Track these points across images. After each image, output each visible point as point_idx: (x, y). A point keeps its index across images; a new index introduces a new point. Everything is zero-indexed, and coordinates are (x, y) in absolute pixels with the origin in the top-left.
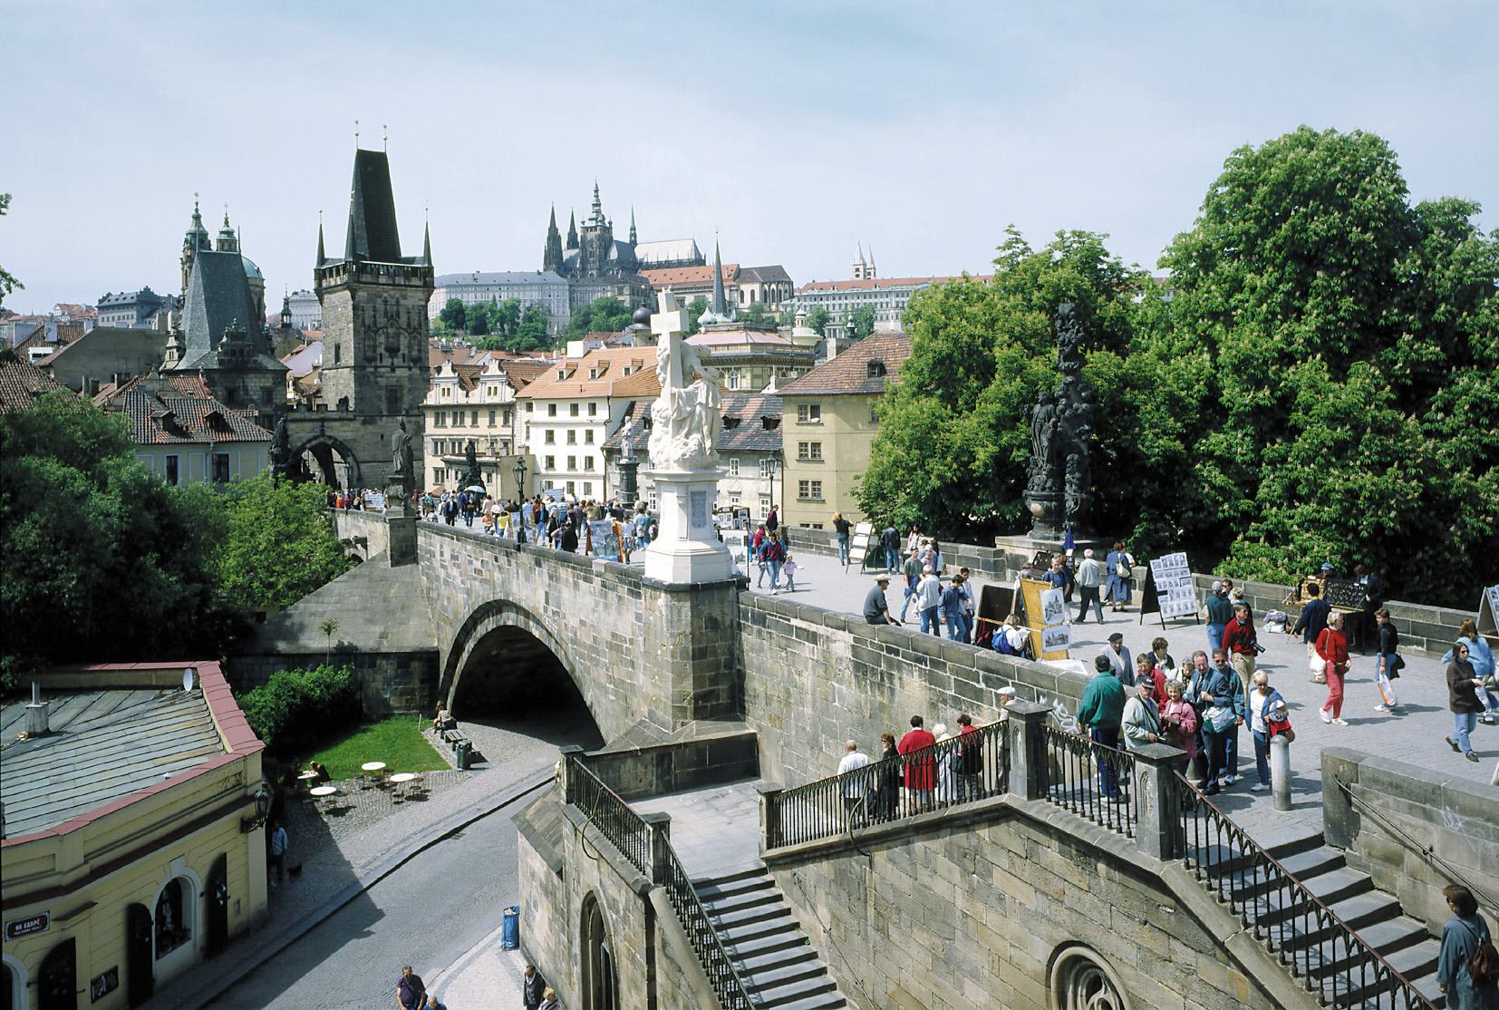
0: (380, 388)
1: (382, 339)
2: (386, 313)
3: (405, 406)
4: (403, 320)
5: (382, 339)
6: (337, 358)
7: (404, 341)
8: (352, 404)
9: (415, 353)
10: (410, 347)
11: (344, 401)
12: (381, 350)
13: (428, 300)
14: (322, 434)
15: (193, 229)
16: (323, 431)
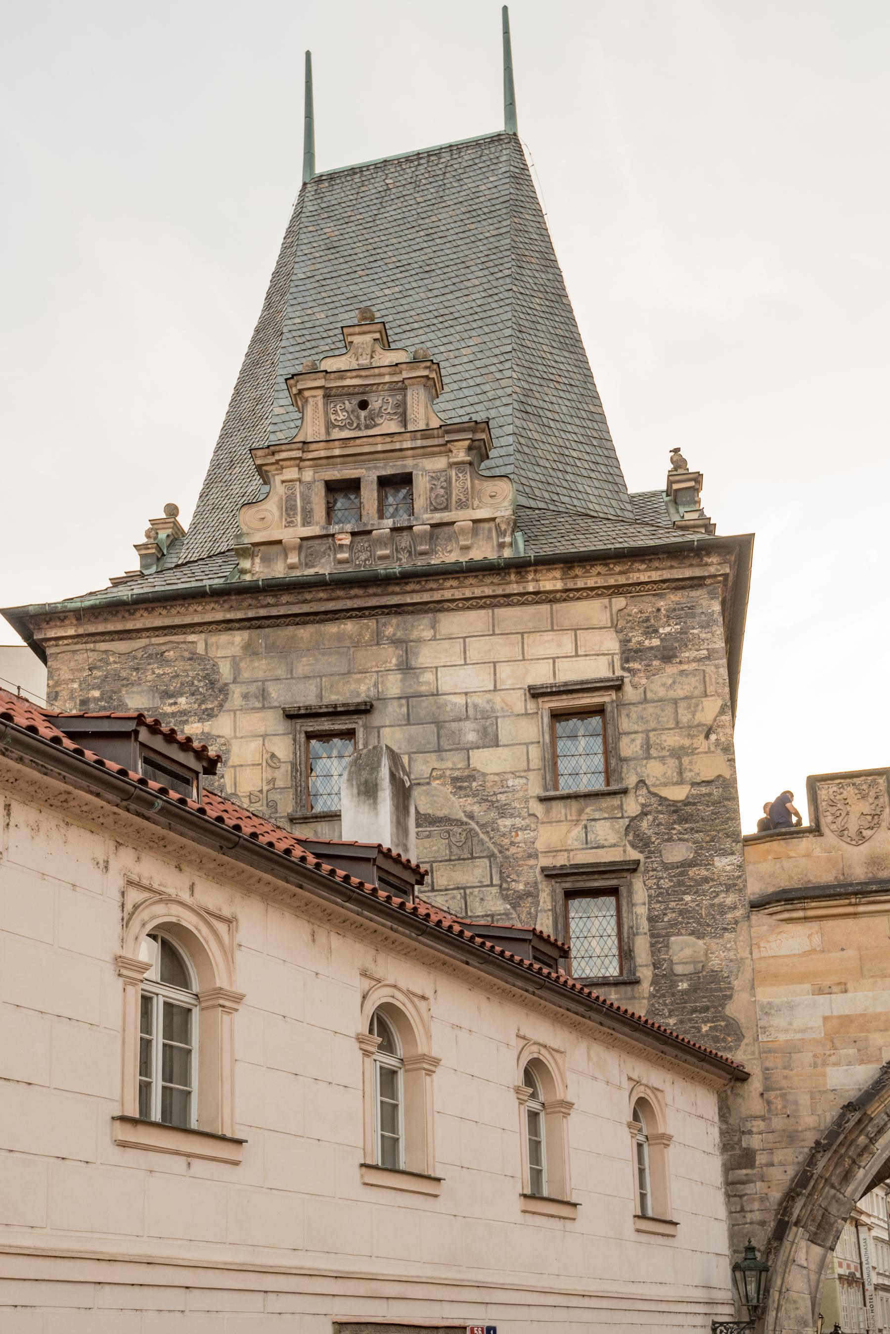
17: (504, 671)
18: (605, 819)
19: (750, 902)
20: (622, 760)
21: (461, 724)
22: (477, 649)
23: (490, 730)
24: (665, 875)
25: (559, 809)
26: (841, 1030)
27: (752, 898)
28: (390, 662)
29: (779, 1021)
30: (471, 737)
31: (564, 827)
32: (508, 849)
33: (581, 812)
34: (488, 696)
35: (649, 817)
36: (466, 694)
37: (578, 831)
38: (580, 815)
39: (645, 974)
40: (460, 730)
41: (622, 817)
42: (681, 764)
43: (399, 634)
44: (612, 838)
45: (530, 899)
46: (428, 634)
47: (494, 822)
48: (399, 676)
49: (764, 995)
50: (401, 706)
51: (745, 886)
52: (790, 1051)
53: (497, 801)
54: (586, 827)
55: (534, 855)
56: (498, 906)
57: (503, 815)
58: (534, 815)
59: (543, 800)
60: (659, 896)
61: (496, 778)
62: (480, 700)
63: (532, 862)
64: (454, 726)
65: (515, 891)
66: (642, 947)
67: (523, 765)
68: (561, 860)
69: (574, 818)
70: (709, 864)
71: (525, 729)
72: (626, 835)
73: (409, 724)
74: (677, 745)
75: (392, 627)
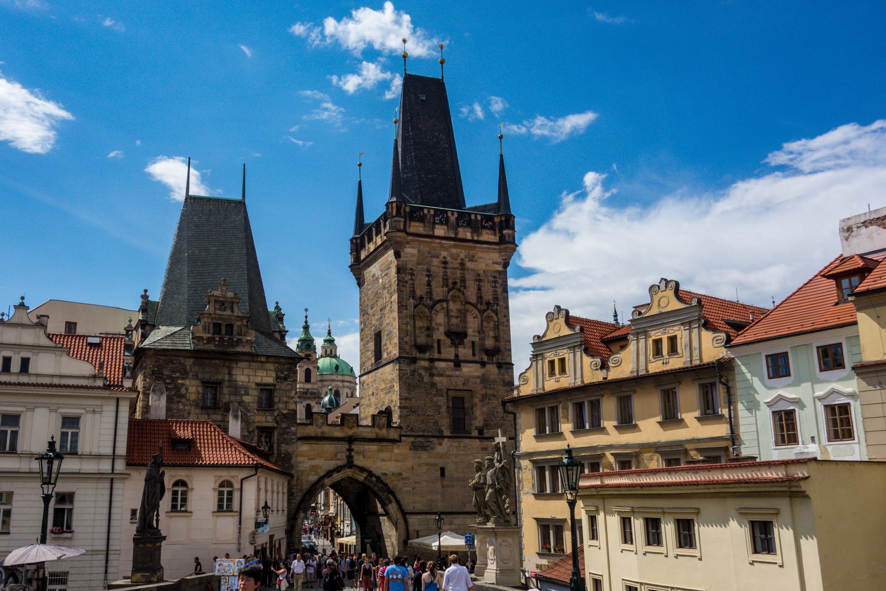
0: (439, 393)
1: (440, 318)
2: (445, 279)
3: (478, 422)
4: (471, 294)
5: (440, 318)
6: (378, 354)
7: (473, 324)
8: (396, 418)
9: (489, 343)
10: (481, 331)
11: (388, 413)
12: (439, 334)
13: (506, 265)
14: (350, 464)
16: (350, 458)
17: (251, 378)
25: (261, 413)
26: (313, 468)
29: (301, 465)
39: (276, 452)
49: (299, 459)
52: (302, 472)
56: (246, 434)
60: (280, 435)
66: (275, 445)
68: (260, 425)
71: (254, 393)
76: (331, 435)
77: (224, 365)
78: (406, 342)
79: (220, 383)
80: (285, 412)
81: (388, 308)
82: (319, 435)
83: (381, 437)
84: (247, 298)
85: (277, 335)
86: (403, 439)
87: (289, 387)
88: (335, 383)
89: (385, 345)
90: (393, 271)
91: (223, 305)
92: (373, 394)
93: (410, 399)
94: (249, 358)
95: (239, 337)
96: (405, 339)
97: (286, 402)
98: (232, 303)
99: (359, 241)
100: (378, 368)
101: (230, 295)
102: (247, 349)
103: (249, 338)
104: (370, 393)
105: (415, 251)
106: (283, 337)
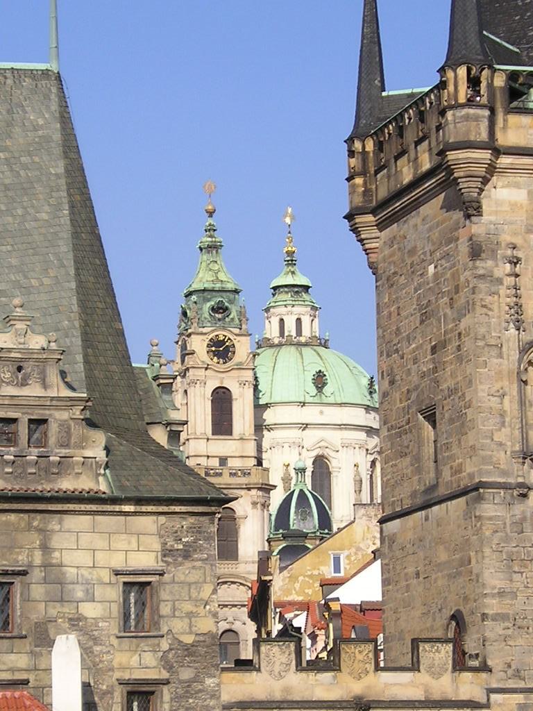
15: (203, 280)
17: (99, 555)
18: (150, 651)
19: (223, 706)
20: (163, 617)
21: (74, 586)
22: (85, 539)
23: (90, 591)
24: (180, 686)
27: (223, 703)
28: (36, 543)
30: (80, 594)
31: (128, 654)
32: (98, 665)
33: (138, 646)
34: (90, 570)
35: (173, 652)
36: (78, 567)
37: (136, 658)
38: (137, 648)
40: (74, 589)
41: (159, 651)
42: (191, 622)
43: (41, 526)
44: (154, 663)
45: (109, 695)
46: (57, 527)
47: (91, 647)
48: (41, 553)
50: (41, 571)
51: (220, 696)
53: (93, 635)
54: (140, 655)
55: (112, 669)
57: (95, 644)
58: (112, 645)
59: (118, 637)
60: (177, 698)
61: (93, 621)
62: (85, 572)
63: (110, 673)
64: (71, 586)
65: (101, 690)
67: (107, 614)
69: (134, 649)
70: (202, 682)
72: (161, 661)
73: (45, 583)
74: (190, 610)
75: (37, 521)
76: (307, 696)
77: (29, 527)
78: (501, 444)
79: (24, 573)
80: (188, 639)
81: (451, 347)
82: (278, 696)
83: (436, 696)
84: (78, 342)
85: (159, 435)
86: (493, 697)
87: (195, 576)
88: (311, 436)
89: (448, 447)
90: (464, 248)
91: (20, 369)
92: (418, 574)
93: (514, 595)
94: (94, 507)
95: (64, 452)
96: (495, 439)
97: (190, 615)
98: (46, 360)
99: (370, 145)
100: (426, 506)
101: (37, 342)
102: (84, 483)
103: (88, 453)
104: (411, 570)
105: (520, 196)
106: (174, 436)
